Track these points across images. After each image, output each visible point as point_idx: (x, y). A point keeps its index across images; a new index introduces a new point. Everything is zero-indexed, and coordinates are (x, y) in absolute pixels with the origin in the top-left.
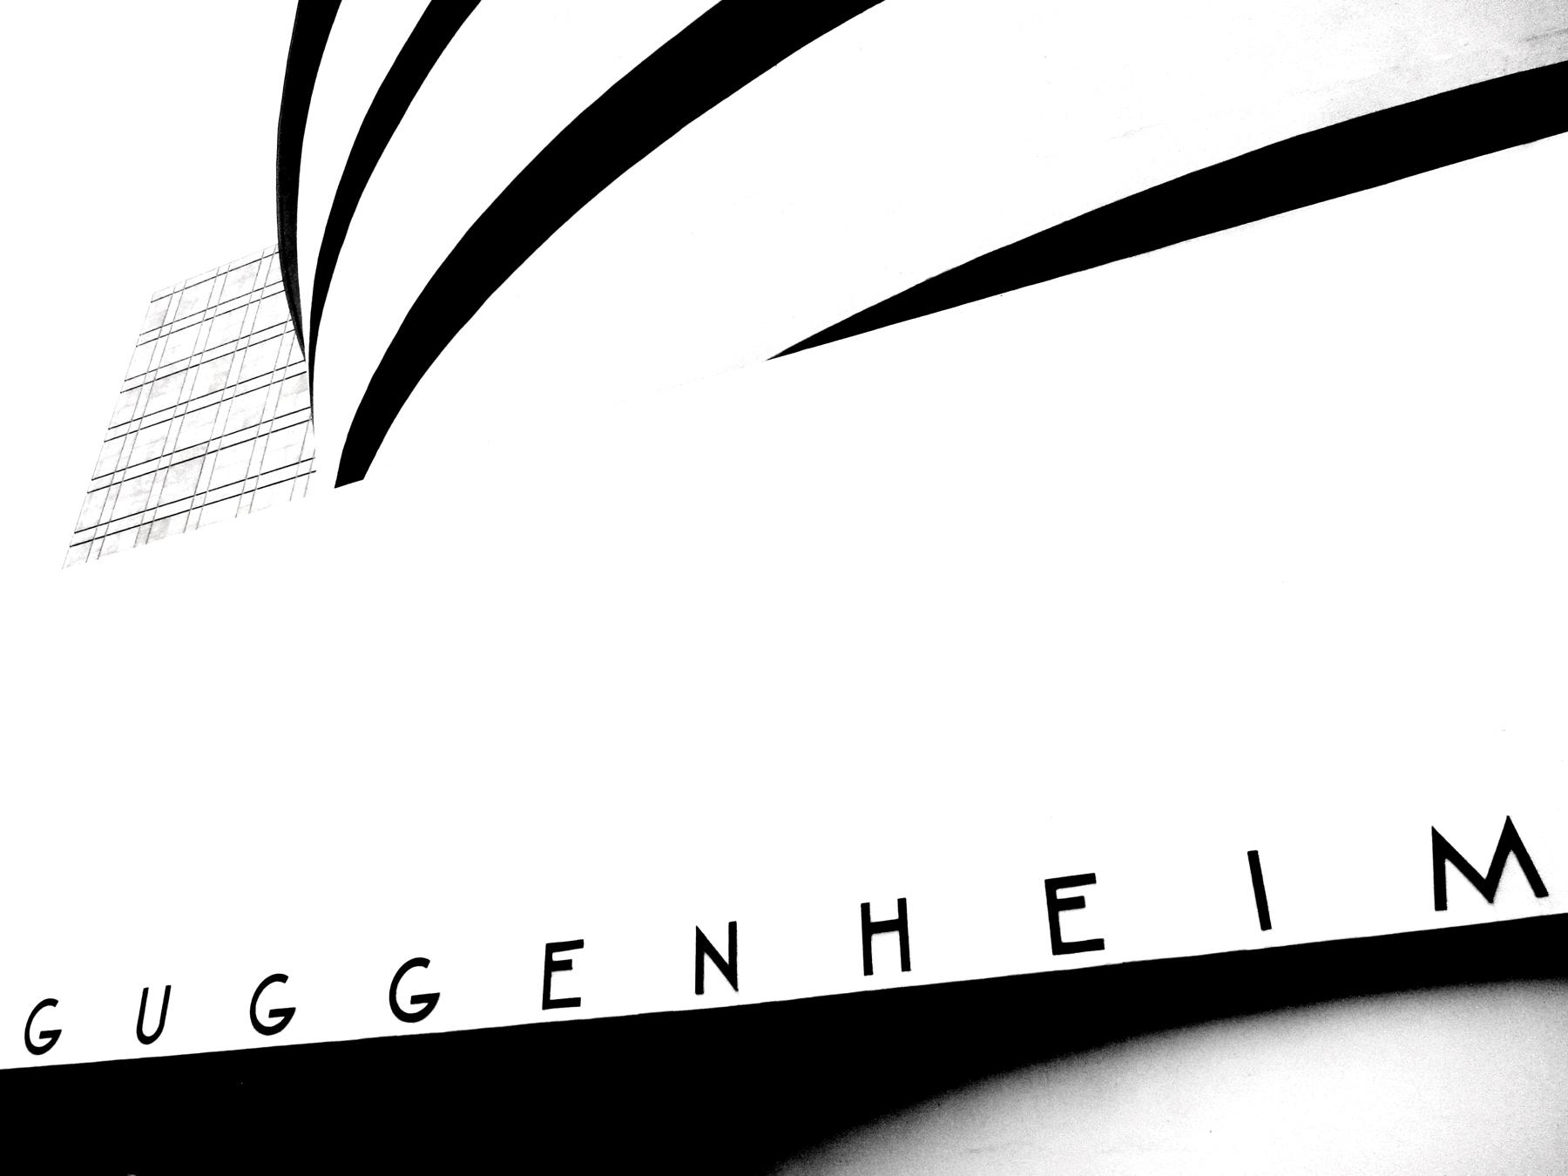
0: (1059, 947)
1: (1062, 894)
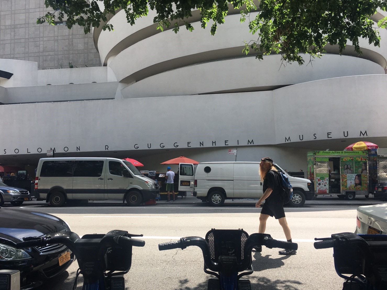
0: (225, 145)
1: (226, 141)
